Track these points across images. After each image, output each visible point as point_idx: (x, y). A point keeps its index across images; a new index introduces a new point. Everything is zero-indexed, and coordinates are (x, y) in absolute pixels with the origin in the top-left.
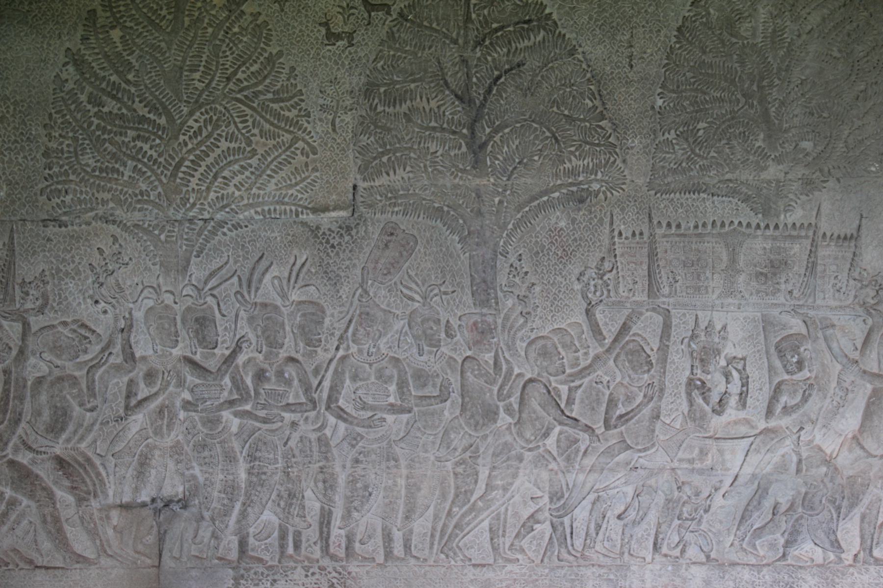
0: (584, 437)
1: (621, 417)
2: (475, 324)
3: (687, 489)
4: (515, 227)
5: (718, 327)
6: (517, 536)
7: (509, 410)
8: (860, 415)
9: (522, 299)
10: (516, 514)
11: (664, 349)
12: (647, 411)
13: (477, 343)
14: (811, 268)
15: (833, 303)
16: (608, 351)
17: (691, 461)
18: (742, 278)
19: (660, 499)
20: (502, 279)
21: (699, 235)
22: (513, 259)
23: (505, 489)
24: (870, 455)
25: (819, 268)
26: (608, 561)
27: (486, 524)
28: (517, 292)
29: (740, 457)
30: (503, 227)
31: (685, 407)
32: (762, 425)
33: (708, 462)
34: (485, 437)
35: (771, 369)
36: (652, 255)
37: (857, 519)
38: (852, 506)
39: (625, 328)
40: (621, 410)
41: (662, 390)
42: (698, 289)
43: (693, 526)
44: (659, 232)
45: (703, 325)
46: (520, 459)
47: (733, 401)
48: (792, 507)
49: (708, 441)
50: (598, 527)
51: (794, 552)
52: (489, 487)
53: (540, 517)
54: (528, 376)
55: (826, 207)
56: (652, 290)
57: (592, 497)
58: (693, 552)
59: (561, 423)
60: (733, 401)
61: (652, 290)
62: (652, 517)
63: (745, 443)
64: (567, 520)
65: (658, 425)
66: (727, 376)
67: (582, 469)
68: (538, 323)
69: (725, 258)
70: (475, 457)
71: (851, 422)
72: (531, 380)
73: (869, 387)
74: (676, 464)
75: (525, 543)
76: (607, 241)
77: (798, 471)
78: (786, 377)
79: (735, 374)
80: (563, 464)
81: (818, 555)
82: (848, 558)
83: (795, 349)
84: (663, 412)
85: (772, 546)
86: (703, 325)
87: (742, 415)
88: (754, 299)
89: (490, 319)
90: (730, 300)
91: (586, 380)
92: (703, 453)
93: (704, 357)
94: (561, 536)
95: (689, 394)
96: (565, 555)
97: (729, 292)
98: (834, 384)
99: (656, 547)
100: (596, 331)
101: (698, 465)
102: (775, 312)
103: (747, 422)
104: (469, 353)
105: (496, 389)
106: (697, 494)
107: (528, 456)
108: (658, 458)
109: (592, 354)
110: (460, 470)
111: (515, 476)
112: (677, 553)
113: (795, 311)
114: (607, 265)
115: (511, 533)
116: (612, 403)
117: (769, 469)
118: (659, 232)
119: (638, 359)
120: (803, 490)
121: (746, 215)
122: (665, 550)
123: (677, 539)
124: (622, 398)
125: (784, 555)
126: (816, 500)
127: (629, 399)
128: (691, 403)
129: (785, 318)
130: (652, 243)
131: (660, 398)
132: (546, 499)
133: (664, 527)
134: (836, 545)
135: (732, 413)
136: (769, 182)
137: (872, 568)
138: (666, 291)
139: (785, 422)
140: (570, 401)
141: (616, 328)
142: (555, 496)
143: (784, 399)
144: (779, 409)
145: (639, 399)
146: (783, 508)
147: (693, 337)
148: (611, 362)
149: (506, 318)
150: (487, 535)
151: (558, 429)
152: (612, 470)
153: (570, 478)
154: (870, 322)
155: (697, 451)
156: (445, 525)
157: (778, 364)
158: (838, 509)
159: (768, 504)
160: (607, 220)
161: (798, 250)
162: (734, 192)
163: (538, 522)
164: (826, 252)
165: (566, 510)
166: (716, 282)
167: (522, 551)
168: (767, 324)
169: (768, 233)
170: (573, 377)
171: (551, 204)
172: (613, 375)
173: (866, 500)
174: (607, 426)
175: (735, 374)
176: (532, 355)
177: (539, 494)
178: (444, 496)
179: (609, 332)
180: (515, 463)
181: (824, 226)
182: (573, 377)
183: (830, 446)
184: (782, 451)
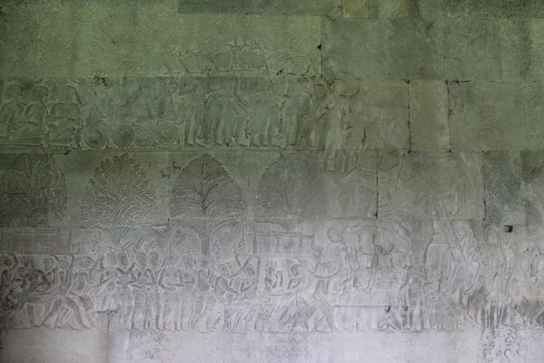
0: (234, 295)
1: (245, 289)
2: (203, 260)
3: (265, 311)
4: (215, 232)
5: (274, 262)
6: (214, 324)
7: (212, 286)
8: (314, 288)
9: (217, 253)
10: (214, 317)
11: (258, 269)
12: (253, 287)
13: (203, 266)
14: (301, 245)
15: (307, 256)
16: (242, 269)
17: (266, 302)
18: (281, 248)
19: (257, 313)
20: (211, 247)
21: (268, 235)
22: (214, 241)
23: (211, 310)
24: (317, 300)
25: (303, 245)
26: (241, 332)
27: (205, 320)
28: (215, 251)
29: (280, 301)
30: (211, 232)
31: (264, 286)
32: (287, 291)
33: (271, 302)
34: (205, 294)
35: (289, 275)
36: (255, 241)
37: (313, 319)
38: (311, 315)
39: (247, 262)
40: (246, 286)
41: (258, 281)
42: (268, 251)
43: (266, 321)
44: (257, 234)
45: (270, 261)
46: (215, 301)
47: (278, 284)
48: (295, 316)
49: (271, 296)
50: (238, 321)
51: (295, 329)
52: (206, 309)
53: (221, 318)
54: (218, 276)
55: (304, 228)
56: (255, 251)
57: (237, 312)
58: (266, 329)
59: (228, 290)
60: (278, 284)
61: (255, 251)
62: (254, 319)
63: (281, 297)
64: (229, 319)
65: (256, 291)
66: (277, 276)
67: (234, 304)
68: (221, 260)
69: (276, 242)
70: (202, 300)
71: (312, 290)
72: (219, 277)
73: (317, 280)
74: (261, 303)
75: (216, 326)
76: (242, 237)
77: (297, 305)
78: (294, 277)
79: (279, 276)
80: (228, 303)
81: (302, 329)
82: (310, 330)
83: (296, 269)
84: (258, 287)
85: (289, 327)
86: (270, 261)
87: (281, 288)
88: (284, 254)
89: (207, 259)
90: (277, 254)
91: (235, 278)
92: (269, 299)
93: (270, 271)
94: (227, 324)
95: (266, 282)
96: (228, 330)
97: (277, 252)
98: (307, 279)
99: (255, 328)
100: (239, 263)
101: (268, 303)
102: (290, 258)
103: (282, 291)
104: (201, 269)
105: (208, 280)
106: (267, 312)
107: (218, 300)
108: (256, 301)
109: (237, 270)
110: (197, 304)
111: (214, 306)
112: (261, 329)
113: (296, 258)
114: (242, 244)
115: (212, 323)
116: (243, 284)
117: (288, 304)
118: (257, 234)
119: (251, 271)
120: (298, 311)
121: (282, 229)
122: (258, 328)
123: (261, 325)
124: (246, 283)
125: (292, 330)
126: (301, 313)
127: (248, 283)
128: (266, 284)
129: (293, 260)
130: (255, 237)
131: (257, 283)
132: (223, 313)
133: (258, 322)
134: (307, 327)
135: (278, 288)
136: (288, 220)
137: (317, 333)
138: (259, 251)
139: (293, 290)
140: (231, 284)
141: (244, 262)
142: (226, 312)
143: (293, 284)
144: (291, 287)
145: (251, 283)
146: (292, 316)
147: (267, 265)
148: (243, 272)
149: (212, 259)
150: (205, 323)
151: (227, 292)
152: (242, 305)
153: (230, 307)
154: (317, 261)
155: (267, 299)
156: (193, 320)
157: (291, 273)
158: (308, 316)
159: (288, 315)
160: (242, 230)
161: (297, 240)
162: (278, 223)
163: (220, 320)
164: (305, 240)
165: (229, 316)
166: (273, 249)
167: (215, 328)
168: (288, 261)
169: (289, 235)
170: (231, 277)
171: (225, 225)
172: (243, 276)
173: (315, 313)
174: (241, 291)
175: (279, 276)
176: (220, 270)
177: (221, 311)
178: (192, 312)
179: (242, 263)
180: (214, 302)
181: (304, 233)
182: (231, 277)
183: (306, 298)
184: (292, 299)
